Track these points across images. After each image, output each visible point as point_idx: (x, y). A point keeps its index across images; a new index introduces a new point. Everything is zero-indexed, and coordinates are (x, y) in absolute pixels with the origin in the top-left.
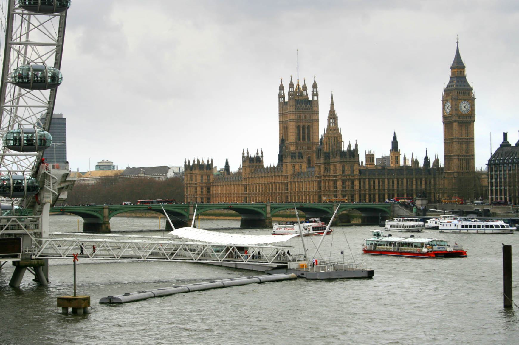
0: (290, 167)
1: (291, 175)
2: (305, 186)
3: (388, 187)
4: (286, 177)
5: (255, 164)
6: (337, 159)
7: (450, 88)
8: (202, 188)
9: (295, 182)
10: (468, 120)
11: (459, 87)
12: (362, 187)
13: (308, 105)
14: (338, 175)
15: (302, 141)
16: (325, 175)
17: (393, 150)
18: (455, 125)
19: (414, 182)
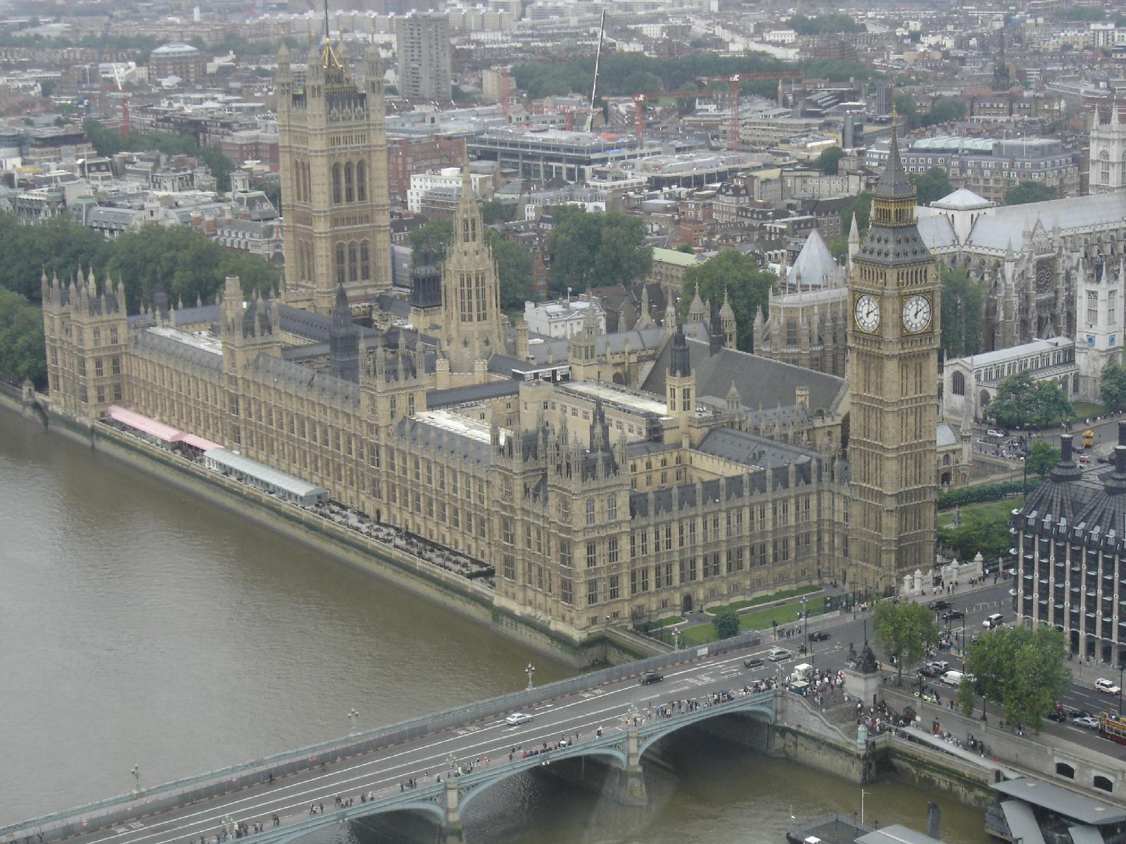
0: (383, 406)
1: (387, 427)
2: (438, 477)
3: (705, 539)
4: (374, 429)
5: (259, 339)
6: (574, 484)
7: (874, 257)
8: (99, 364)
9: (403, 452)
10: (925, 348)
11: (902, 258)
12: (636, 550)
13: (359, 107)
14: (577, 532)
15: (344, 204)
16: (526, 507)
17: (678, 374)
18: (891, 368)
19: (769, 513)
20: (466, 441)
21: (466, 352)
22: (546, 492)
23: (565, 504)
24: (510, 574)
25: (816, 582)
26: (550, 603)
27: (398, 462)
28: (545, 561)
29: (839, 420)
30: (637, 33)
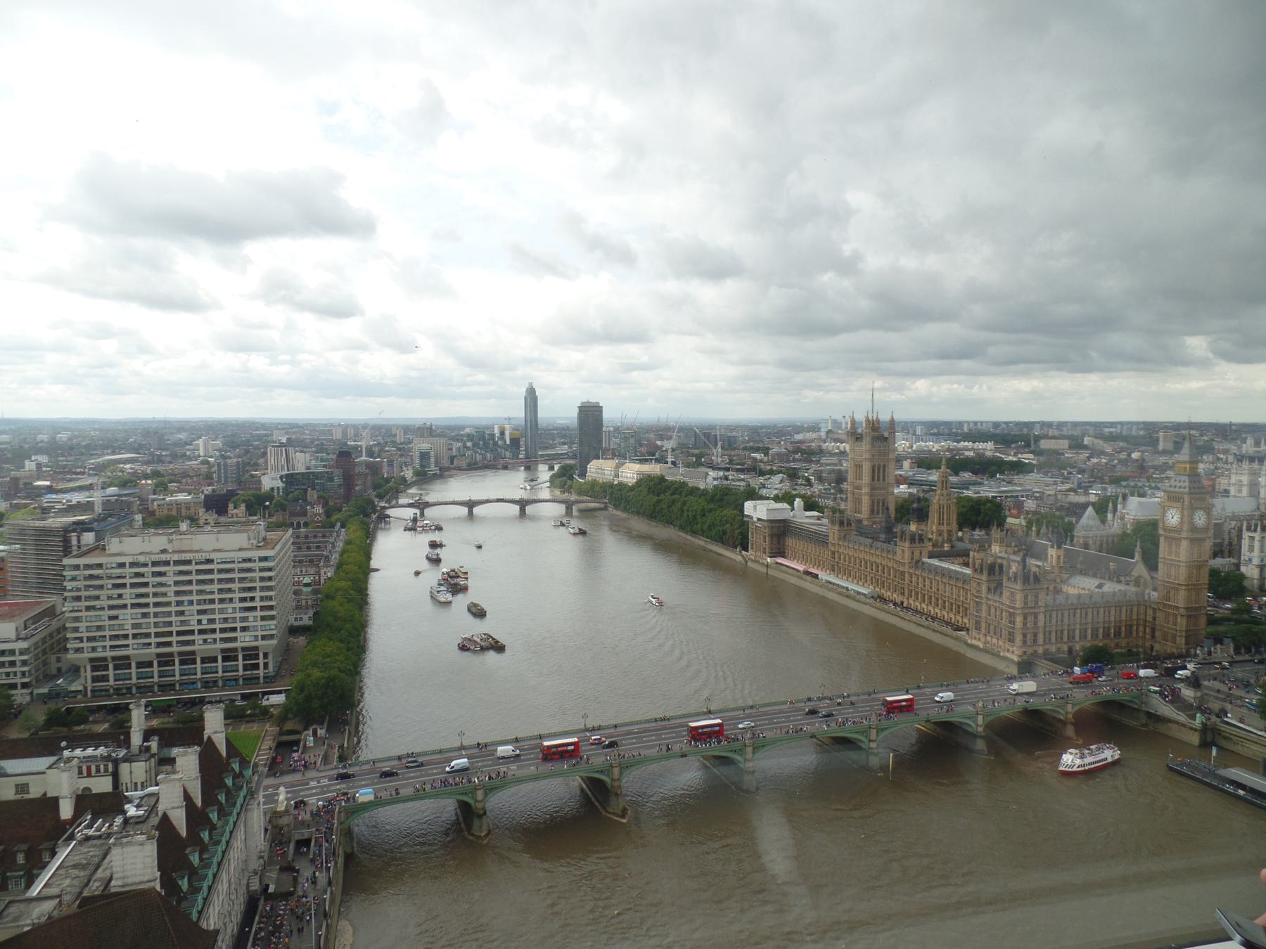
0: (907, 554)
4: (903, 564)
6: (1018, 586)
7: (1177, 490)
15: (876, 482)
16: (989, 597)
17: (1055, 546)
18: (1184, 544)
20: (951, 571)
21: (940, 539)
22: (1001, 589)
23: (1012, 594)
24: (978, 629)
25: (1135, 650)
26: (1001, 643)
27: (914, 579)
28: (999, 623)
29: (1133, 579)
30: (963, 454)
